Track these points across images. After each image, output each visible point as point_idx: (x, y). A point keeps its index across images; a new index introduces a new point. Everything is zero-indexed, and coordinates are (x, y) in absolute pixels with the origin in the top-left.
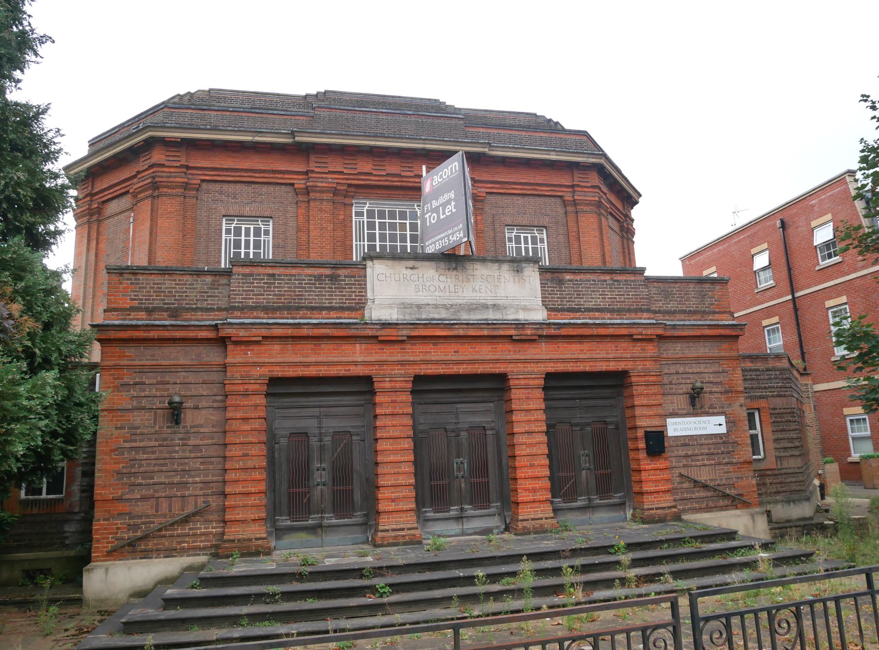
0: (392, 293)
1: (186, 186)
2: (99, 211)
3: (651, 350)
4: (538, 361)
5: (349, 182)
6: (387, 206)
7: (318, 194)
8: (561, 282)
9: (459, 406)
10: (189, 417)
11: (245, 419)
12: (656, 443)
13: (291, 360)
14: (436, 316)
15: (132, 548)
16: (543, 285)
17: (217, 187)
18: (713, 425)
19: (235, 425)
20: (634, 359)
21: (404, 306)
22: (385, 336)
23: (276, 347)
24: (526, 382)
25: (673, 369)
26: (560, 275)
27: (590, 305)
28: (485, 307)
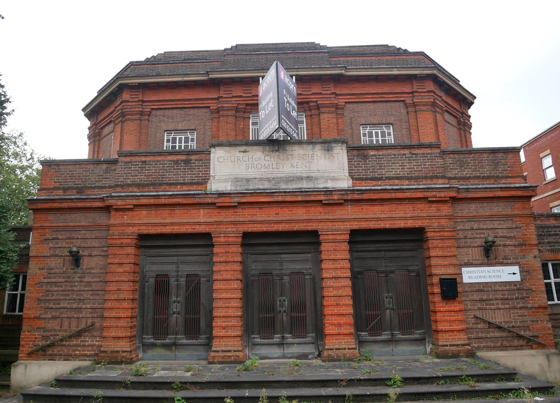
0: (229, 170)
1: (142, 113)
2: (99, 134)
3: (446, 209)
4: (343, 221)
5: (246, 102)
7: (225, 112)
8: (365, 157)
9: (283, 256)
10: (85, 262)
11: (121, 264)
12: (451, 288)
13: (153, 221)
14: (261, 187)
15: (43, 352)
16: (350, 160)
17: (162, 112)
18: (508, 274)
19: (113, 268)
20: (430, 217)
21: (237, 180)
22: (222, 203)
23: (144, 212)
24: (334, 237)
25: (468, 226)
26: (365, 152)
27: (391, 174)
28: (301, 179)
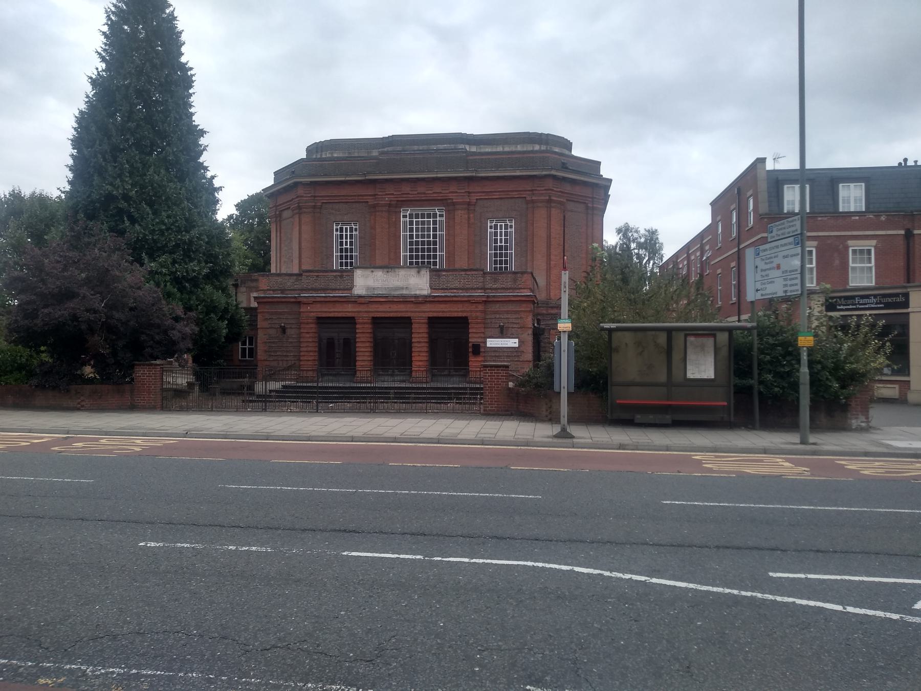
0: (366, 282)
1: (314, 207)
2: (280, 215)
3: (481, 307)
4: (424, 312)
6: (419, 210)
8: (439, 276)
10: (288, 332)
12: (477, 349)
18: (512, 343)
19: (304, 335)
20: (471, 311)
21: (368, 288)
22: (359, 301)
23: (319, 305)
25: (493, 316)
28: (402, 288)
